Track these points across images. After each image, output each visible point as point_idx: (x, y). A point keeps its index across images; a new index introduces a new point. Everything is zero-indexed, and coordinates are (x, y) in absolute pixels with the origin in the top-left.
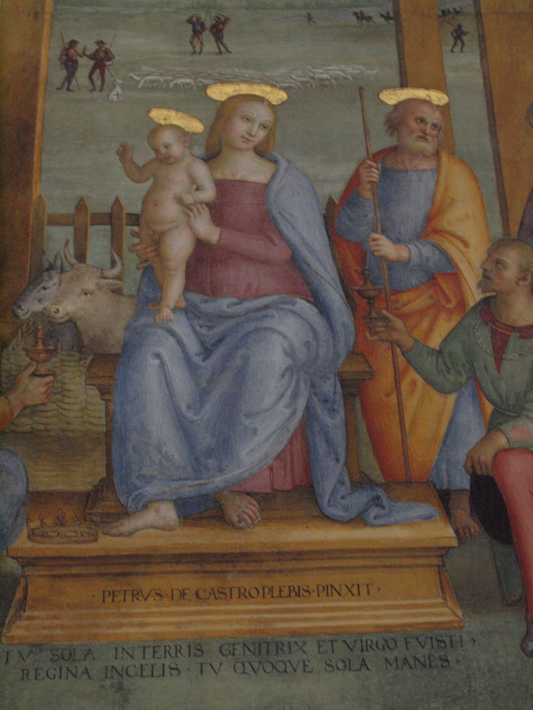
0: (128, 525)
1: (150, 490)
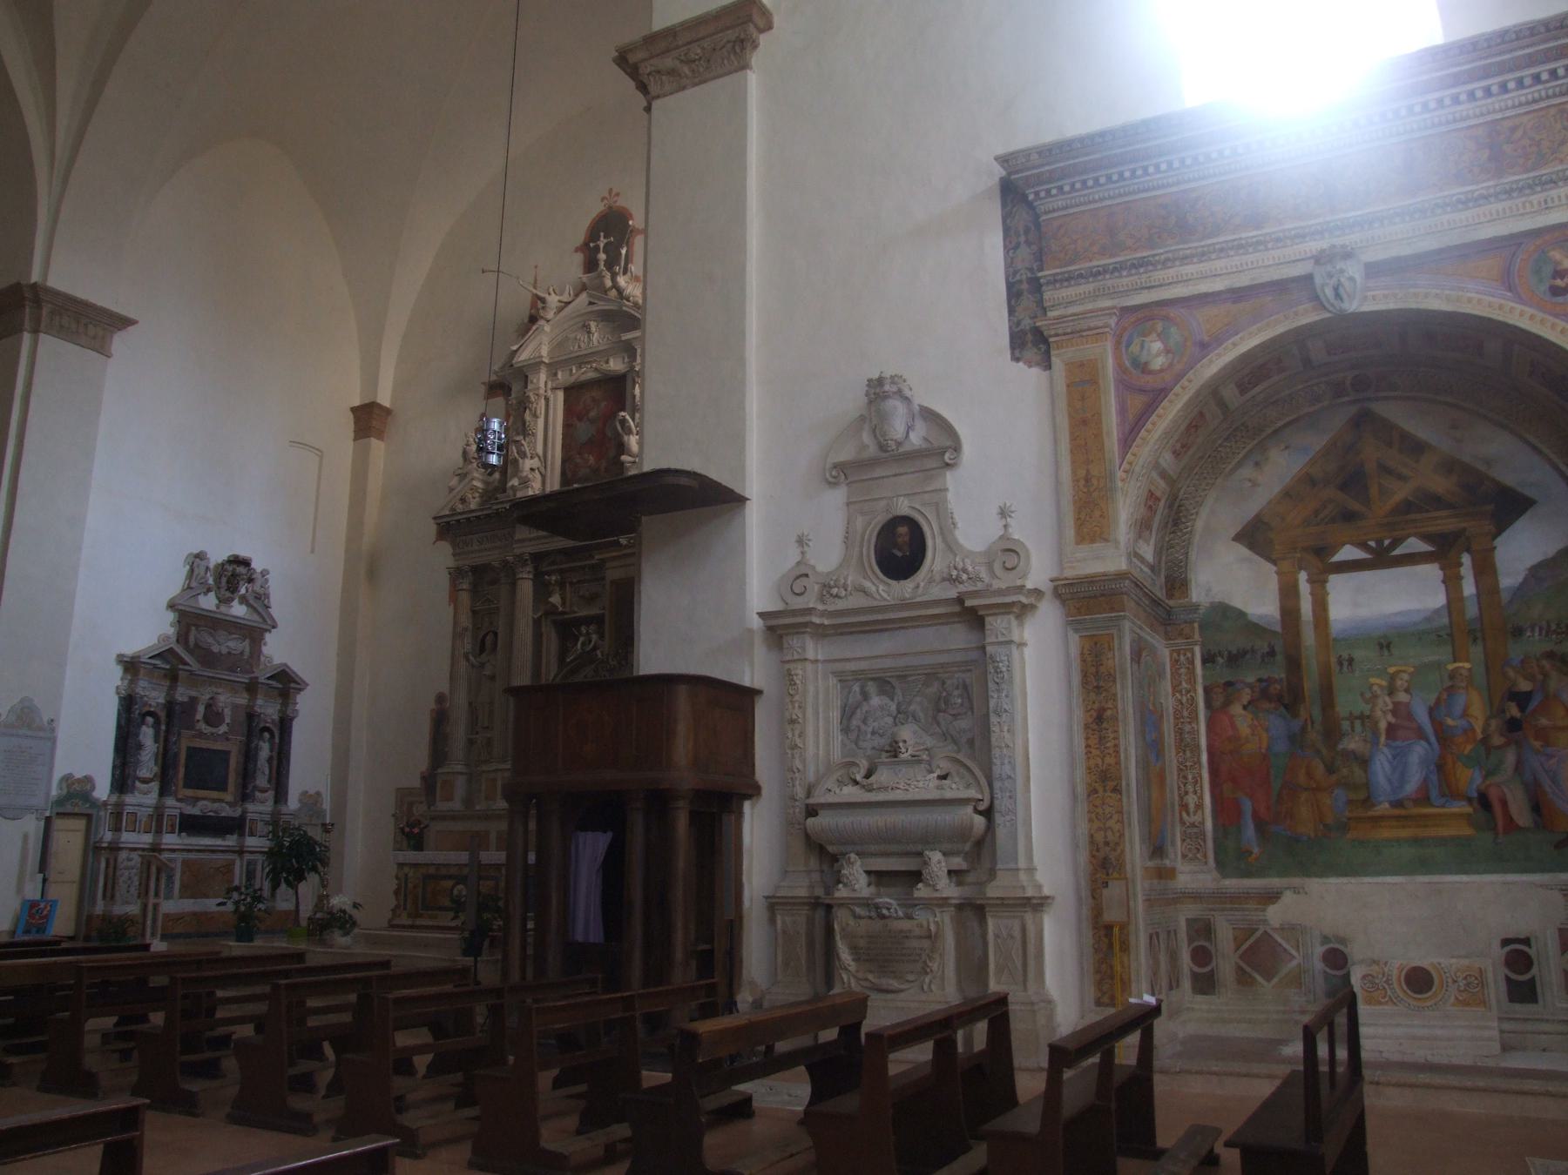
0: (1376, 809)
1: (1381, 799)
